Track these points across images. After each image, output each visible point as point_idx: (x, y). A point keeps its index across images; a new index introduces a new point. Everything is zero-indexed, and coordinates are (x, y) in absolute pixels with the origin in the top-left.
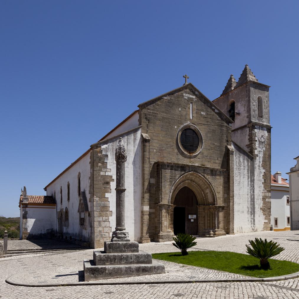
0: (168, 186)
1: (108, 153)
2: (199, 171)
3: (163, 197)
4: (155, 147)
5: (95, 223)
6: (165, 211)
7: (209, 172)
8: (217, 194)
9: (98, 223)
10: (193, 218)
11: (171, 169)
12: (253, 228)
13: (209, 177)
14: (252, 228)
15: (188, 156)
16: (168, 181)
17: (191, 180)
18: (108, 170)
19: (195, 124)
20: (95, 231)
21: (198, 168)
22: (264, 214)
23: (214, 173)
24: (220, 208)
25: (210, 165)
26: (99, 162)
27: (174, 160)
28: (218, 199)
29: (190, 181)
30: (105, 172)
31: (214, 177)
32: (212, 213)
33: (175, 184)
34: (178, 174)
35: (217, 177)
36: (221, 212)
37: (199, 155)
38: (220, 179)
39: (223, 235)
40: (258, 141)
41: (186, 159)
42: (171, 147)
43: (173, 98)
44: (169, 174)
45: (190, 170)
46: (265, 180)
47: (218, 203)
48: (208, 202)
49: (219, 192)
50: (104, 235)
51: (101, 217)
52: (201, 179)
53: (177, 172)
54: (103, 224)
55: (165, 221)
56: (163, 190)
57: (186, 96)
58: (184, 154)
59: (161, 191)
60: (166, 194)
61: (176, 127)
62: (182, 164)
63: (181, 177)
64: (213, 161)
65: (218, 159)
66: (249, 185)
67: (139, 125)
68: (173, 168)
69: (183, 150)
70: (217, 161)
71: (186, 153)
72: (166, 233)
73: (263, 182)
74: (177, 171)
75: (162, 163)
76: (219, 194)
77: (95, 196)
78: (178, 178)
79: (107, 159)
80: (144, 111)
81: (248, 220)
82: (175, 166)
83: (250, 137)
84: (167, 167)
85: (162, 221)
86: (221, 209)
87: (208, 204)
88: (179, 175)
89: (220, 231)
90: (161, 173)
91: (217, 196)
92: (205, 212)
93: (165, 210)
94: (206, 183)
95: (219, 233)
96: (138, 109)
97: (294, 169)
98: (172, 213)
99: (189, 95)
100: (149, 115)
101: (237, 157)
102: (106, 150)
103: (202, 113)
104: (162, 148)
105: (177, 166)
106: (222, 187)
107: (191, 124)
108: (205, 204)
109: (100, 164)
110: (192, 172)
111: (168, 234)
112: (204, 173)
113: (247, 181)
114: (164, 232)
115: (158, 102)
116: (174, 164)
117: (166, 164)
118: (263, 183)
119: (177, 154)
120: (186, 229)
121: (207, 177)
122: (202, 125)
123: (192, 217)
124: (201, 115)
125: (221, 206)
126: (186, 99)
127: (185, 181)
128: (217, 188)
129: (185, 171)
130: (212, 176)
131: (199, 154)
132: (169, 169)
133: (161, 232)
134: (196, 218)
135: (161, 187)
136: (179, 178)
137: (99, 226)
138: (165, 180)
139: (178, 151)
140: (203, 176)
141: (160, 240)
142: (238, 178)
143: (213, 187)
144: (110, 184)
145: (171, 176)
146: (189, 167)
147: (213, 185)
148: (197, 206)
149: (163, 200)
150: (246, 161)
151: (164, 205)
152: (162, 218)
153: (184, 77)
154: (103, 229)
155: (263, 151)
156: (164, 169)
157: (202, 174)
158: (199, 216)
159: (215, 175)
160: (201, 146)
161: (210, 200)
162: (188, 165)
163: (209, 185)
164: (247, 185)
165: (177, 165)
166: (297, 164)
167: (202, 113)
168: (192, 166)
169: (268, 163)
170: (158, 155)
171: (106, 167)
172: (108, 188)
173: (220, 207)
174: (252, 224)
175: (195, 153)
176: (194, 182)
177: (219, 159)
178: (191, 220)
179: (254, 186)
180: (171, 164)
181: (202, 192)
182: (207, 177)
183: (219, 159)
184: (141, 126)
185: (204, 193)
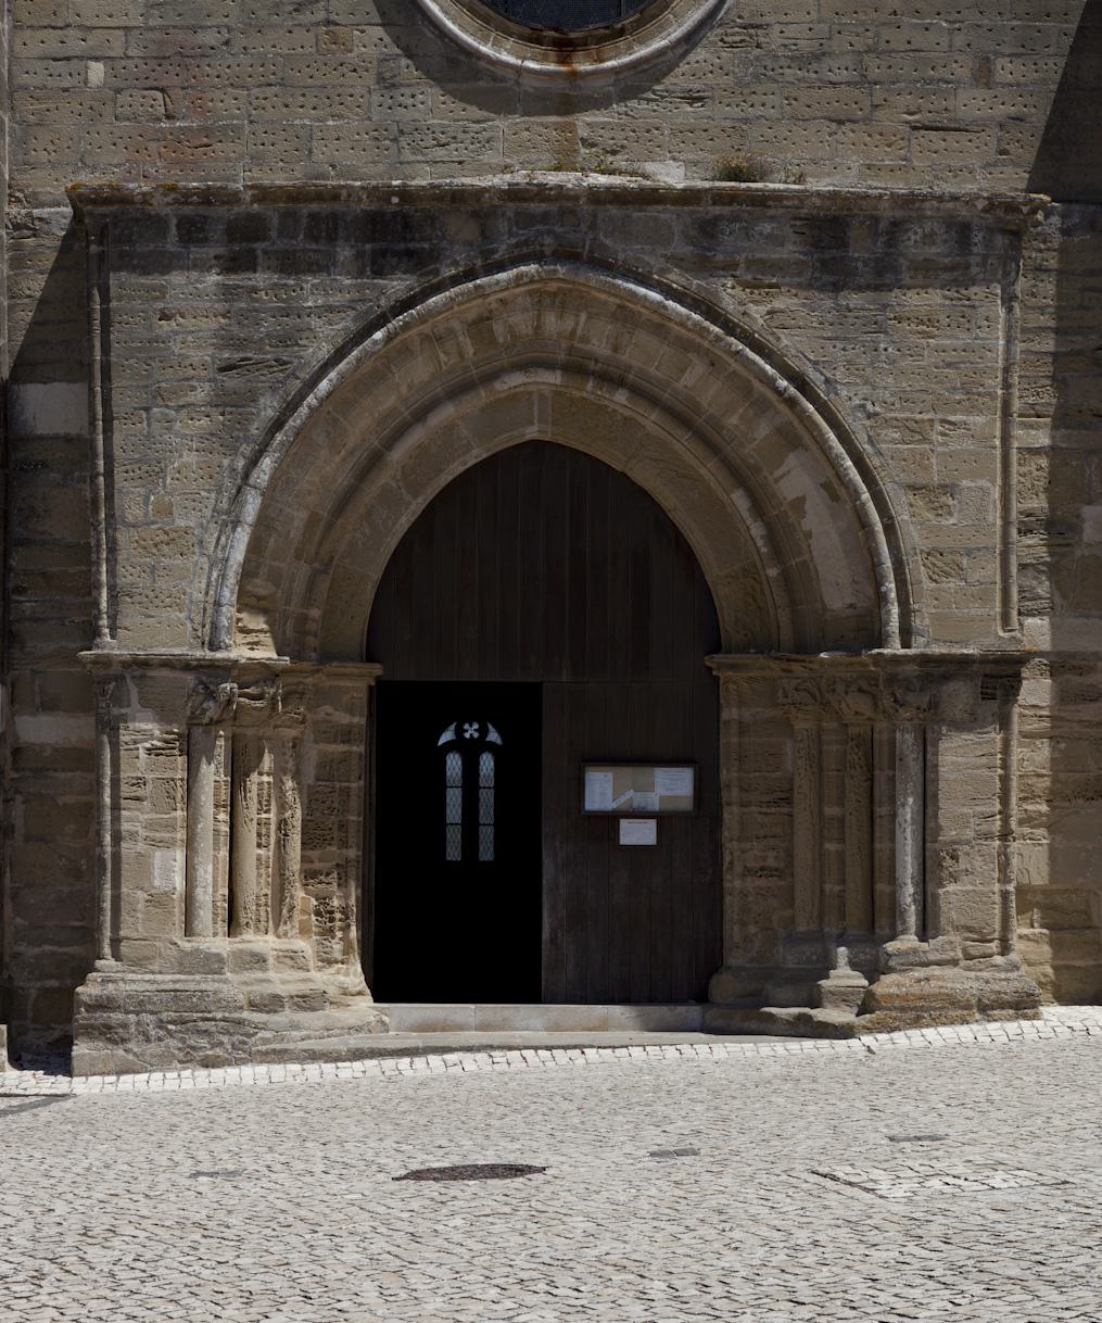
0: (190, 458)
2: (621, 251)
3: (127, 576)
4: (95, 39)
6: (154, 728)
7: (790, 251)
8: (903, 508)
10: (653, 801)
11: (231, 265)
13: (780, 303)
15: (528, 84)
16: (201, 394)
17: (576, 368)
21: (614, 211)
23: (860, 250)
24: (945, 678)
25: (855, 162)
27: (348, 158)
28: (918, 571)
31: (855, 299)
33: (294, 422)
34: (330, 309)
35: (915, 300)
36: (959, 726)
37: (700, 54)
38: (965, 317)
39: (987, 1008)
41: (502, 124)
44: (212, 324)
45: (502, 250)
47: (917, 622)
53: (311, 292)
55: (155, 843)
56: (132, 501)
58: (476, 74)
59: (110, 516)
60: (175, 540)
62: (373, 192)
63: (378, 335)
64: (906, 100)
65: (984, 75)
68: (259, 246)
70: (971, 103)
71: (504, 53)
72: (167, 980)
74: (311, 281)
75: (107, 201)
76: (941, 510)
78: (325, 350)
82: (292, 216)
84: (172, 243)
85: (117, 838)
86: (959, 694)
88: (345, 324)
89: (954, 963)
90: (106, 313)
91: (913, 535)
93: (164, 715)
95: (932, 987)
98: (345, 758)
104: (181, 36)
105: (313, 217)
110: (532, 268)
111: (191, 982)
112: (703, 265)
114: (139, 963)
116: (263, 194)
117: (160, 205)
119: (387, 83)
120: (546, 935)
121: (757, 312)
123: (639, 800)
125: (965, 661)
128: (916, 431)
129: (419, 261)
130: (836, 288)
131: (691, 39)
132: (202, 266)
133: (107, 963)
134: (687, 805)
135: (109, 474)
136: (339, 354)
138: (159, 393)
139: (397, 41)
140: (695, 304)
141: (81, 1049)
143: (845, 438)
145: (239, 344)
146: (475, 214)
147: (846, 400)
148: (712, 661)
149: (130, 615)
151: (141, 665)
152: (116, 807)
156: (133, 269)
157: (676, 278)
158: (728, 774)
159: (884, 276)
161: (837, 593)
162: (458, 197)
165: (314, 207)
168: (514, 194)
170: (135, 118)
173: (941, 670)
175: (642, 42)
177: (1005, 70)
178: (624, 823)
180: (233, 198)
181: (739, 500)
182: (757, 312)
183: (1005, 70)
185: (758, 509)
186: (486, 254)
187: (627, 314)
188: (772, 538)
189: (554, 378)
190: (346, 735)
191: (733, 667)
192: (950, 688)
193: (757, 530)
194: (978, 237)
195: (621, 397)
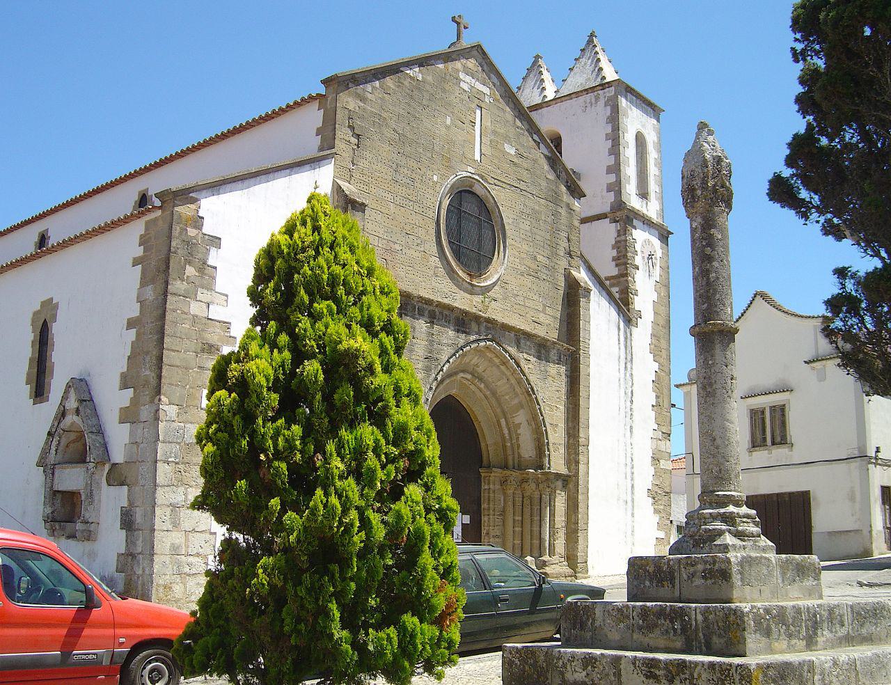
5: (158, 511)
9: (168, 511)
16: (420, 366)
19: (486, 181)
20: (158, 547)
22: (656, 511)
26: (190, 263)
29: (469, 377)
32: (531, 498)
43: (430, 78)
46: (657, 397)
48: (520, 456)
49: (557, 425)
51: (181, 489)
52: (503, 373)
57: (467, 82)
67: (321, 149)
69: (453, 264)
71: (460, 273)
77: (162, 397)
80: (348, 101)
83: (618, 252)
87: (520, 467)
92: (505, 494)
94: (518, 390)
96: (322, 90)
100: (362, 118)
106: (562, 408)
107: (477, 177)
108: (510, 463)
109: (190, 271)
115: (389, 81)
118: (653, 406)
122: (504, 185)
124: (505, 153)
127: (456, 373)
137: (170, 527)
153: (453, 19)
154: (187, 540)
160: (502, 254)
161: (527, 450)
163: (530, 395)
171: (210, 287)
173: (558, 476)
176: (481, 379)
184: (333, 151)
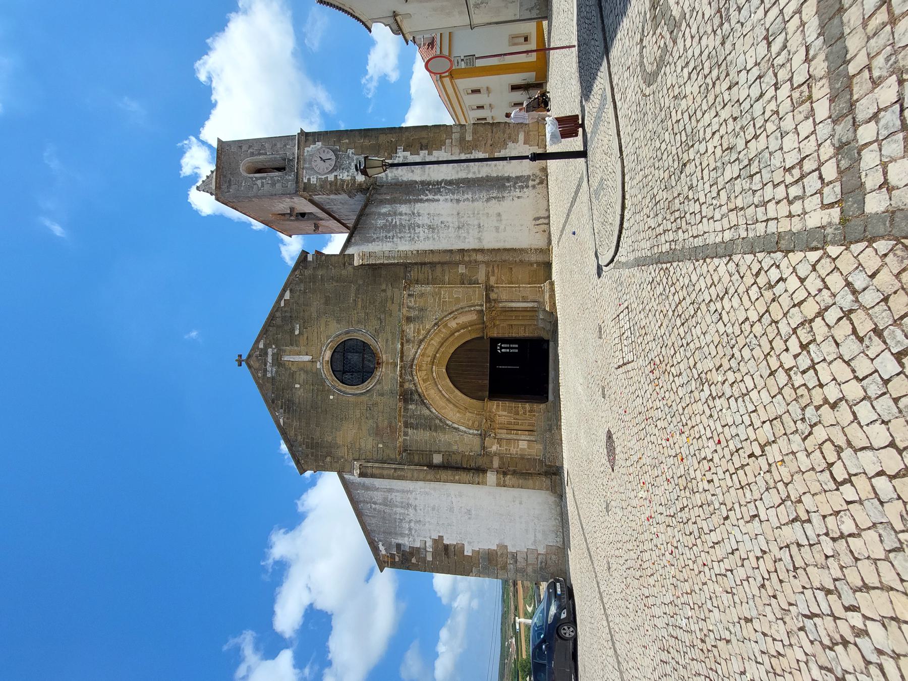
1: (393, 543)
12: (537, 181)
14: (539, 184)
17: (433, 363)
18: (423, 546)
24: (489, 298)
26: (411, 561)
30: (426, 551)
39: (552, 290)
40: (335, 173)
42: (370, 409)
50: (541, 563)
54: (521, 563)
61: (331, 397)
65: (384, 291)
66: (436, 197)
70: (389, 293)
73: (426, 152)
79: (404, 546)
81: (518, 197)
82: (404, 416)
86: (493, 296)
97: (395, 27)
99: (268, 364)
101: (375, 236)
102: (388, 547)
103: (297, 332)
113: (426, 204)
125: (486, 295)
126: (276, 372)
142: (422, 233)
144: (448, 545)
150: (384, 210)
155: (355, 157)
164: (435, 204)
166: (380, 22)
167: (297, 332)
169: (383, 139)
171: (418, 549)
172: (454, 548)
174: (527, 187)
177: (384, 287)
179: (438, 183)
181: (457, 334)
183: (384, 287)
185: (458, 331)
186: (411, 381)
187: (423, 355)
188: (463, 329)
189: (434, 367)
190: (498, 406)
191: (487, 335)
192: (491, 297)
193: (462, 331)
194: (410, 293)
195: (438, 355)
